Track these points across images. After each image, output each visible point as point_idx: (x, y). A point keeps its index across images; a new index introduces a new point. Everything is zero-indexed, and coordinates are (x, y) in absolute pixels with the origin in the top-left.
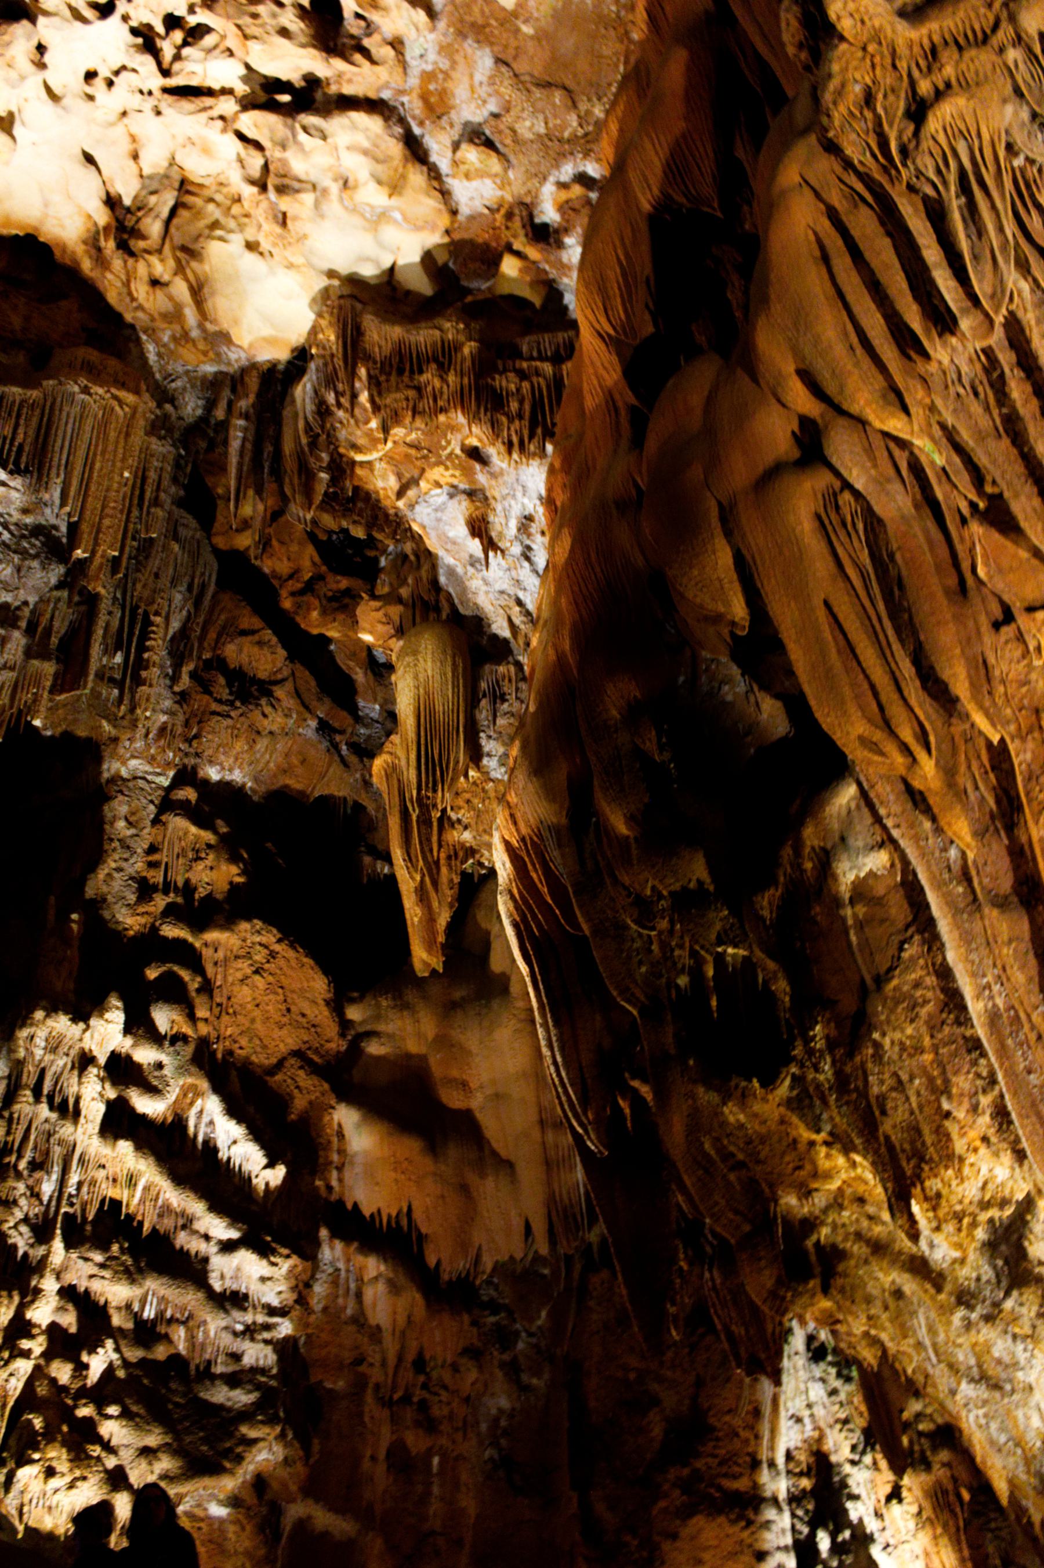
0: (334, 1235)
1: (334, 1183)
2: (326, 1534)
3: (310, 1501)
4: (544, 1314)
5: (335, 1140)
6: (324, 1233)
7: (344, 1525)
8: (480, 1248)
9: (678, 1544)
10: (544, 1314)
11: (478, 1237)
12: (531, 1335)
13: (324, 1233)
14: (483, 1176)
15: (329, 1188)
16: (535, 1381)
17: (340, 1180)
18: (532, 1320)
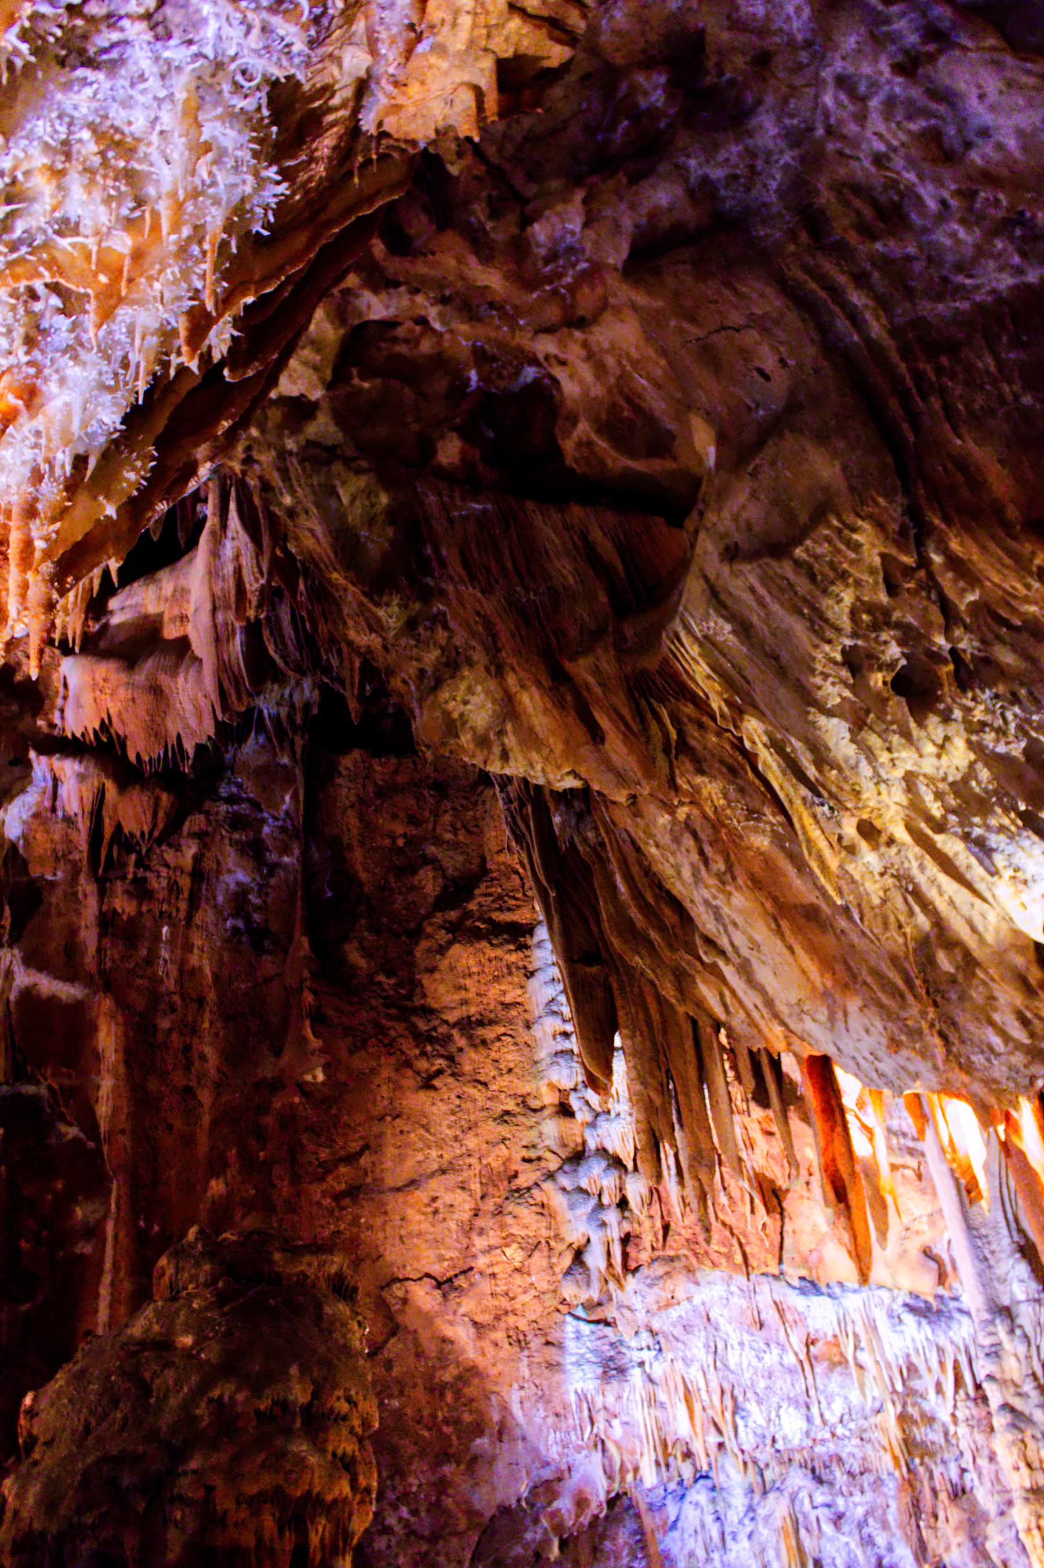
0: (40, 752)
1: (57, 721)
2: (53, 999)
3: (32, 971)
4: (287, 798)
5: (61, 689)
6: (32, 754)
7: (72, 991)
8: (179, 736)
9: (437, 976)
10: (287, 798)
11: (173, 727)
12: (276, 819)
13: (32, 754)
14: (174, 675)
15: (52, 726)
16: (286, 859)
17: (63, 718)
18: (276, 806)
